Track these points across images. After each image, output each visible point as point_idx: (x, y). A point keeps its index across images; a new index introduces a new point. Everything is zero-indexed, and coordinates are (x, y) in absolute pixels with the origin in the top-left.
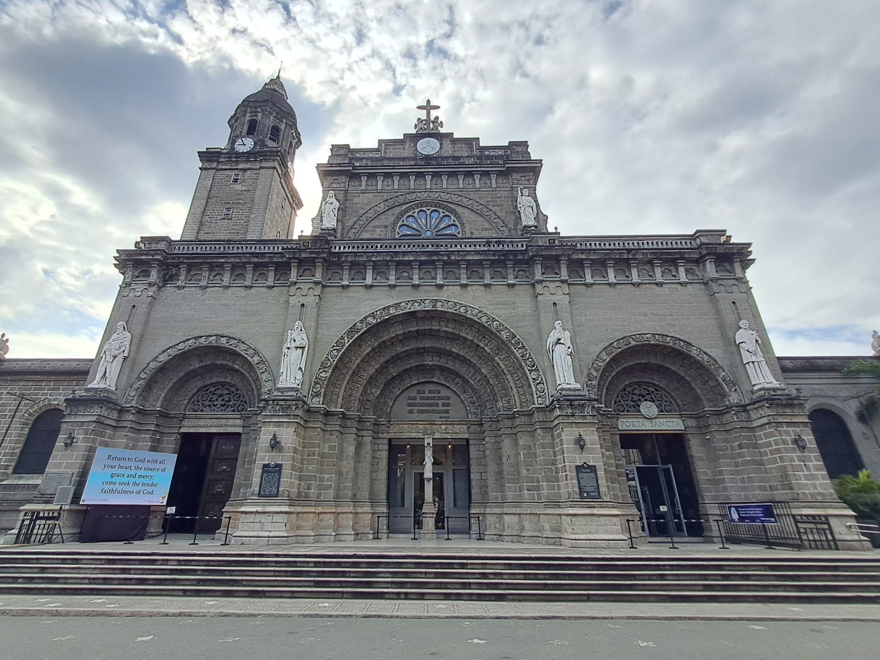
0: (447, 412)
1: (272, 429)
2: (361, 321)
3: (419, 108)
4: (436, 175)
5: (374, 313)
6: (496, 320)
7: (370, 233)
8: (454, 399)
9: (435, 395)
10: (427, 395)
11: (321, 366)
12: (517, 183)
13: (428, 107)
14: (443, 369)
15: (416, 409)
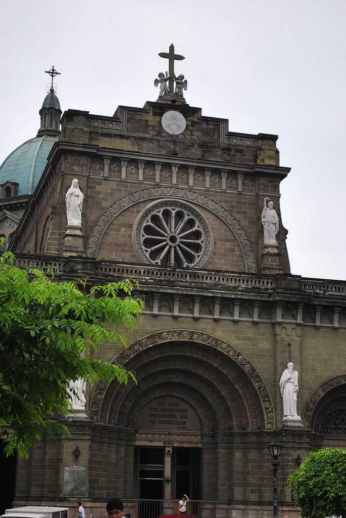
0: (184, 423)
1: (72, 443)
2: (130, 349)
3: (162, 55)
4: (183, 168)
5: (140, 341)
6: (241, 355)
7: (114, 232)
8: (190, 413)
9: (175, 408)
10: (167, 407)
11: (97, 388)
12: (263, 189)
13: (172, 56)
14: (181, 385)
15: (157, 419)
